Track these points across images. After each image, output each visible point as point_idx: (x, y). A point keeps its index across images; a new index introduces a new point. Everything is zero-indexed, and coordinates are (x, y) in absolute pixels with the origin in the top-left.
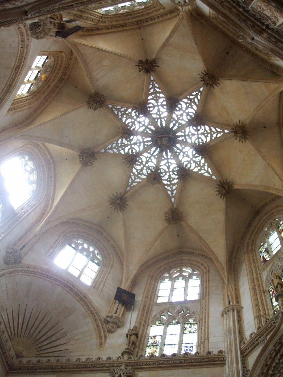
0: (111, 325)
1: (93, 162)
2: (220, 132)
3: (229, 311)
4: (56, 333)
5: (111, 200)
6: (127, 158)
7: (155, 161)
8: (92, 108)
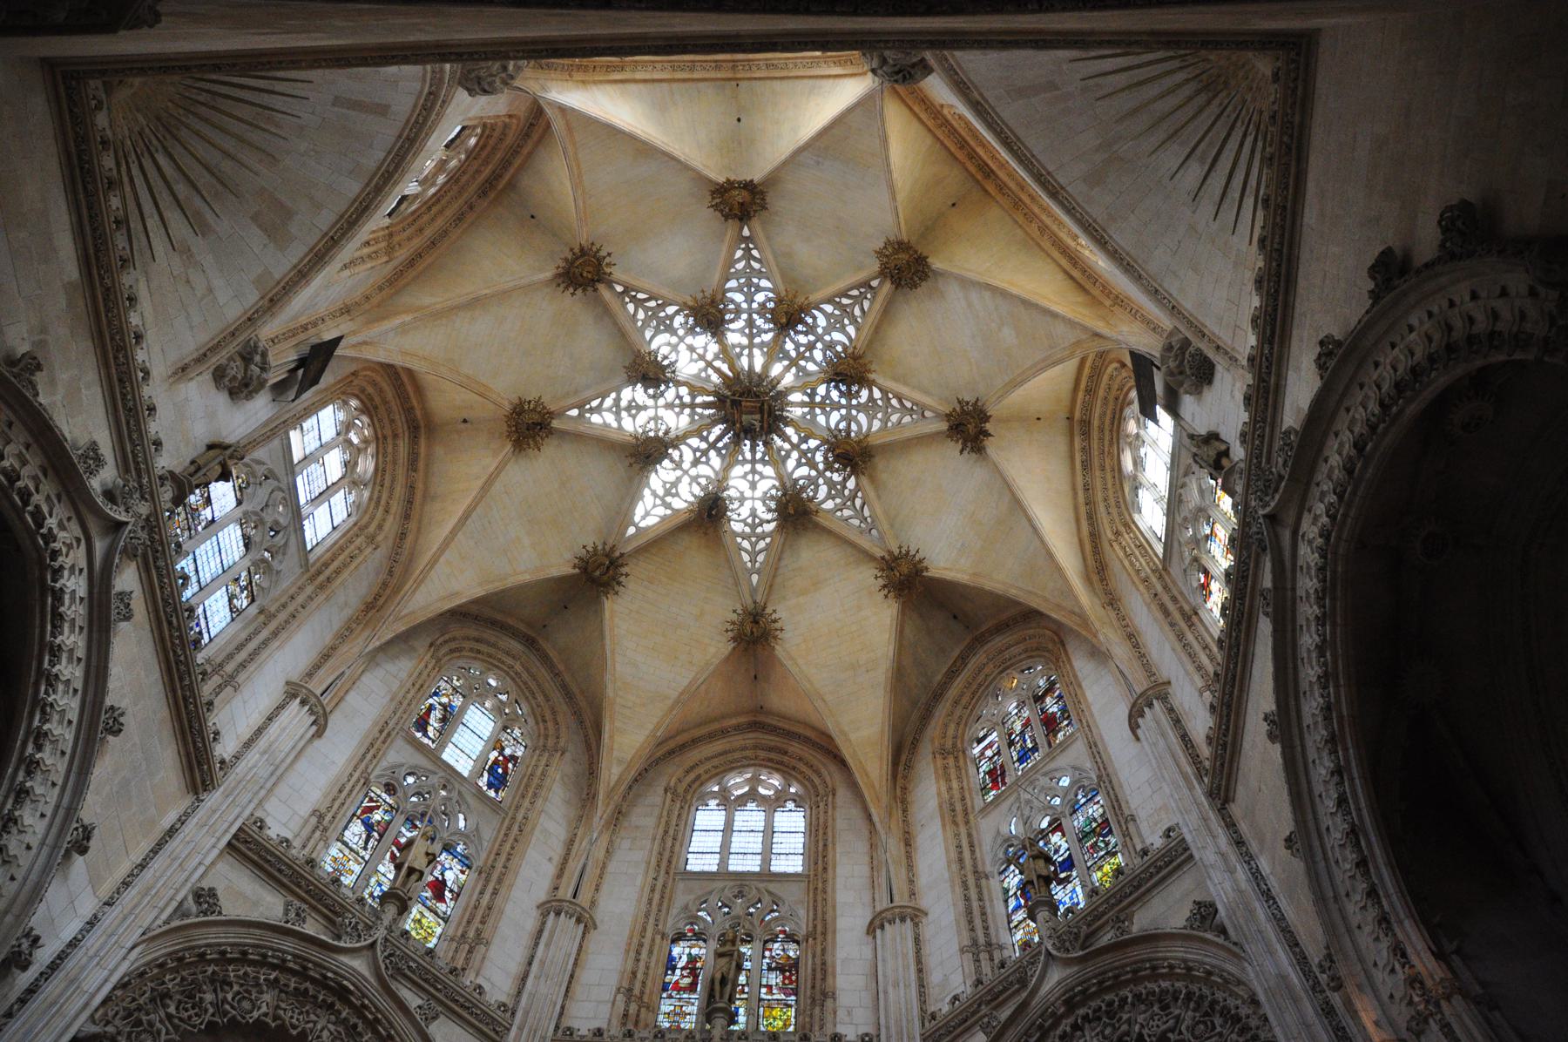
1: (721, 211)
2: (753, 561)
4: (199, 192)
8: (885, 248)
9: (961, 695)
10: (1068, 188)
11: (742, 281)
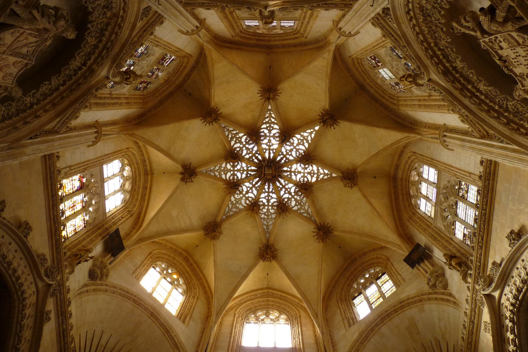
0: (437, 283)
1: (274, 248)
2: (270, 114)
3: (445, 141)
5: (318, 240)
6: (280, 214)
7: (290, 185)
8: (219, 236)
9: (184, 69)
10: (147, 317)
11: (270, 217)
